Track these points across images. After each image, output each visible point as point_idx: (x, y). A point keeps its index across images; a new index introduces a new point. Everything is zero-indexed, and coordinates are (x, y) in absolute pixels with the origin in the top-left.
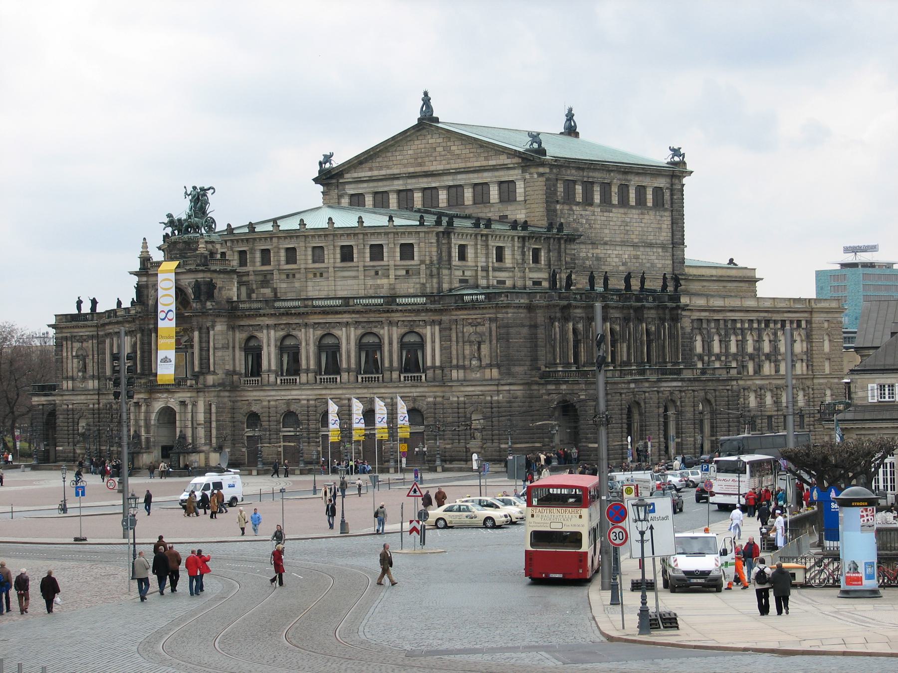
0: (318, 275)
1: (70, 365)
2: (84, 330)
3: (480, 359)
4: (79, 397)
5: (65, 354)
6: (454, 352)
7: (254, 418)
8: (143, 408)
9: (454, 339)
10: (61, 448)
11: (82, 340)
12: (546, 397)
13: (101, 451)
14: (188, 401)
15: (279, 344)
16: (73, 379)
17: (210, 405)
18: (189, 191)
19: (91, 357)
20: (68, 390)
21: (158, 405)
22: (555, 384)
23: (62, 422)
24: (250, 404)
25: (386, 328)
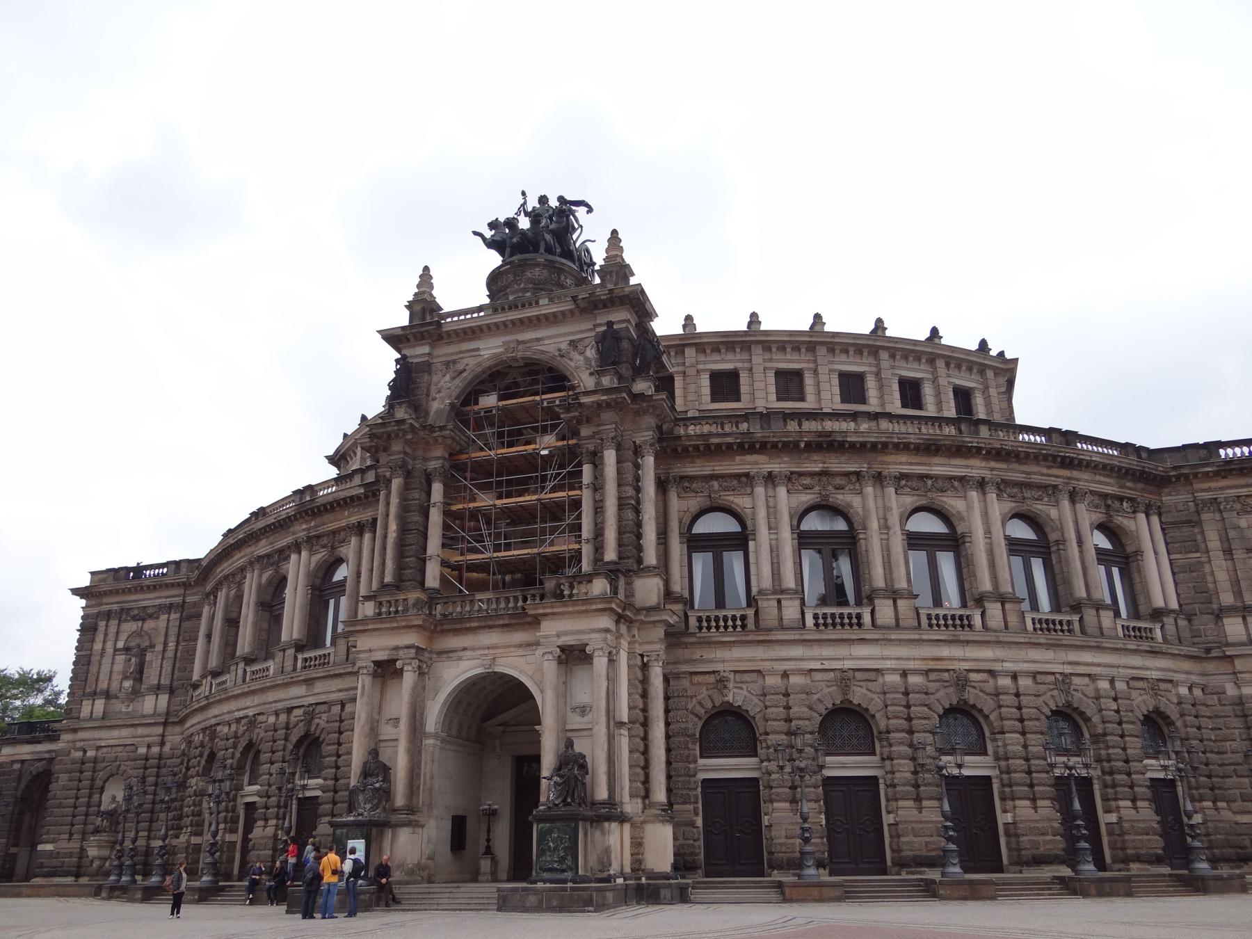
1: (105, 668)
4: (115, 733)
5: (98, 646)
6: (1222, 577)
7: (729, 727)
8: (409, 678)
9: (1214, 541)
10: (49, 847)
11: (144, 615)
13: (148, 852)
14: (595, 643)
15: (795, 523)
16: (107, 695)
17: (645, 667)
18: (532, 203)
19: (159, 648)
21: (455, 673)
23: (65, 788)
24: (721, 683)
25: (1066, 503)
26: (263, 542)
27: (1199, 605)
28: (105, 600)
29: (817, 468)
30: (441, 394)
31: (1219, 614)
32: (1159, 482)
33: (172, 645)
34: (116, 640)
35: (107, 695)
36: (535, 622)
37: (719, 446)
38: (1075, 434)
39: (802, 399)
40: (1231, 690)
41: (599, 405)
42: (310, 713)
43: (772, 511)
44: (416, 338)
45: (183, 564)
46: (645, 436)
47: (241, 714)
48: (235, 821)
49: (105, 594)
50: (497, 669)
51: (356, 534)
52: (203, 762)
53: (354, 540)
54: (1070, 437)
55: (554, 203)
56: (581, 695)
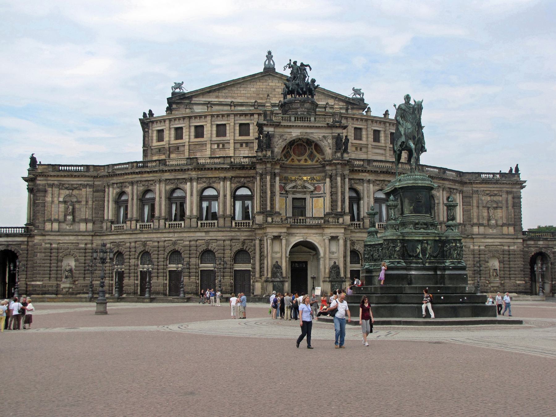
0: (359, 149)
1: (54, 209)
2: (76, 179)
3: (496, 221)
4: (67, 238)
5: (49, 199)
8: (284, 242)
9: (475, 204)
10: (38, 283)
11: (72, 188)
12: (527, 249)
16: (57, 221)
18: (292, 63)
19: (84, 203)
20: (52, 231)
22: (535, 240)
26: (166, 174)
27: (468, 221)
28: (49, 178)
29: (382, 179)
30: (278, 146)
31: (473, 225)
32: (463, 183)
33: (90, 203)
34: (59, 197)
35: (57, 221)
36: (323, 228)
37: (356, 170)
38: (446, 169)
39: (361, 139)
40: (472, 247)
41: (338, 163)
42: (208, 243)
43: (368, 191)
44: (270, 125)
45: (91, 167)
46: (347, 172)
47: (166, 239)
48: (166, 277)
49: (51, 176)
50: (308, 240)
51: (224, 181)
52: (137, 254)
53: (222, 183)
54: (444, 170)
55: (299, 64)
56: (334, 249)
